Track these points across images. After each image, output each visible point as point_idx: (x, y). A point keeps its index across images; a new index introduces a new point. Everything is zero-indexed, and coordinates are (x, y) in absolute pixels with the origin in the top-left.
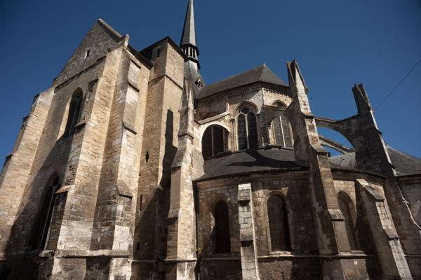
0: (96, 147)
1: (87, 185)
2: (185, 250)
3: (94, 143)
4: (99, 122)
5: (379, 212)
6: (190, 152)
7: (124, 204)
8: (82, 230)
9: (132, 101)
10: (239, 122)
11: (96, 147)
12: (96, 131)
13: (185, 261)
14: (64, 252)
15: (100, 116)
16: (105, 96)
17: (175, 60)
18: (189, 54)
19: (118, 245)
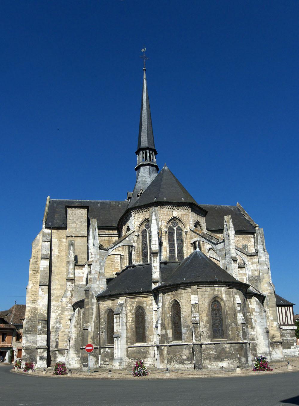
0: (34, 298)
1: (32, 317)
2: (66, 344)
3: (32, 296)
4: (34, 284)
5: (115, 321)
6: (71, 289)
7: (41, 325)
8: (33, 338)
9: (45, 267)
10: (143, 236)
11: (34, 298)
12: (33, 289)
13: (65, 350)
14: (25, 347)
15: (34, 280)
16: (35, 268)
17: (76, 218)
18: (148, 159)
19: (40, 343)
